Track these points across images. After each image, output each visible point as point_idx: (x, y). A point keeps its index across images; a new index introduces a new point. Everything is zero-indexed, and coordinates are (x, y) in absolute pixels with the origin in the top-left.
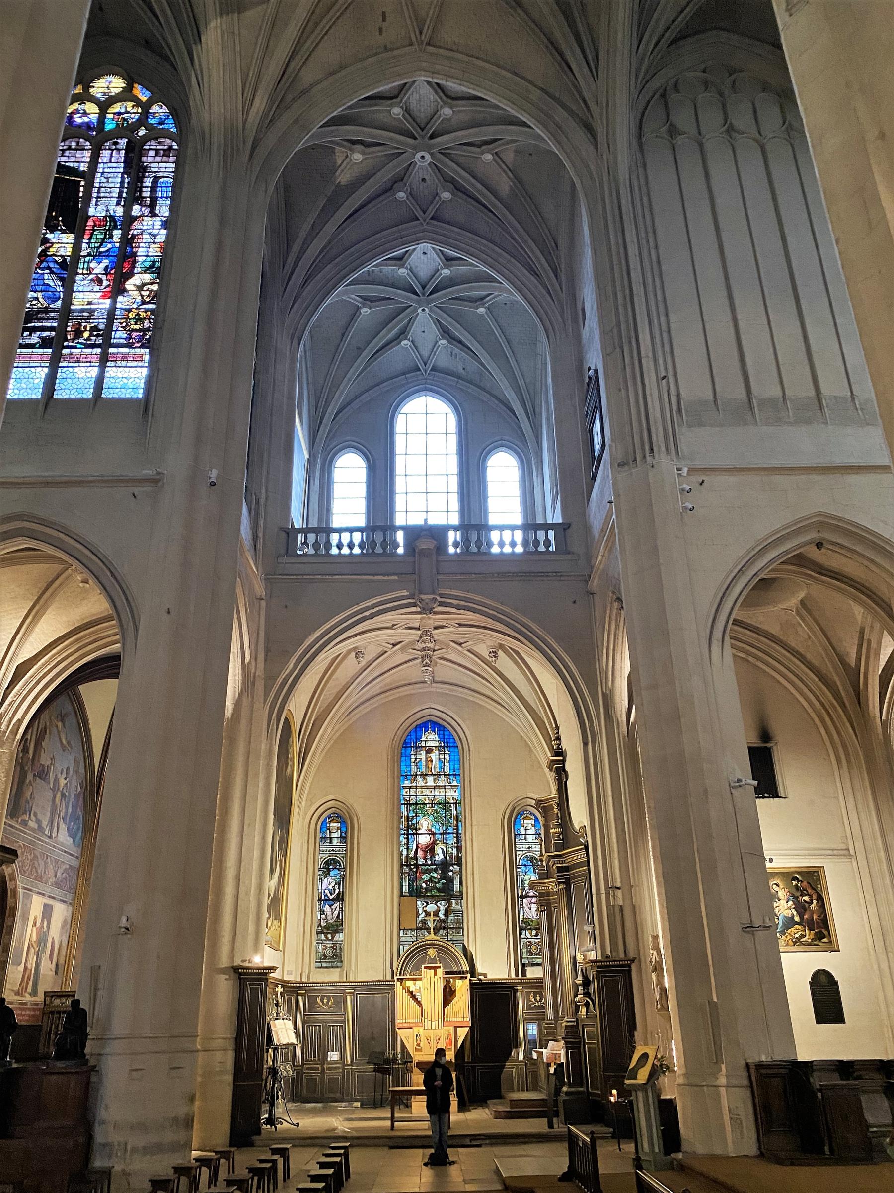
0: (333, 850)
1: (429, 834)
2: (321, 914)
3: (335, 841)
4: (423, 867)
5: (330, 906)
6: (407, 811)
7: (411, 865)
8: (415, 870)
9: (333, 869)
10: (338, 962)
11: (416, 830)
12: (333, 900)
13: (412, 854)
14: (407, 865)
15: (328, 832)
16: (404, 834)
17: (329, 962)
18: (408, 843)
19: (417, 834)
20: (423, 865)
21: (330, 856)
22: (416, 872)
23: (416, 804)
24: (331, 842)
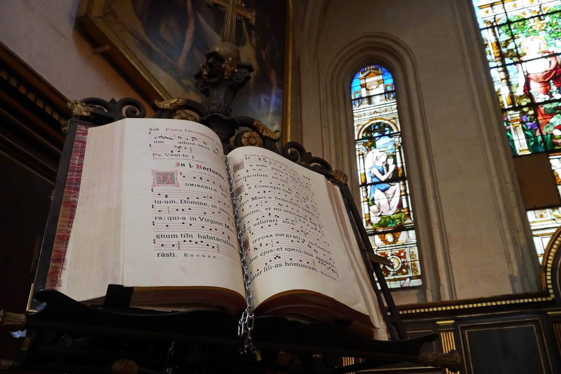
0: (376, 112)
1: (546, 57)
2: (369, 205)
3: (377, 100)
4: (548, 106)
5: (383, 191)
6: (495, 35)
7: (520, 107)
8: (531, 112)
9: (380, 137)
10: (411, 278)
11: (518, 56)
12: (387, 181)
13: (519, 91)
14: (514, 109)
15: (364, 90)
16: (497, 67)
17: (395, 280)
18: (507, 78)
19: (521, 62)
20: (546, 102)
21: (372, 120)
22: (536, 115)
23: (509, 23)
24: (370, 103)
